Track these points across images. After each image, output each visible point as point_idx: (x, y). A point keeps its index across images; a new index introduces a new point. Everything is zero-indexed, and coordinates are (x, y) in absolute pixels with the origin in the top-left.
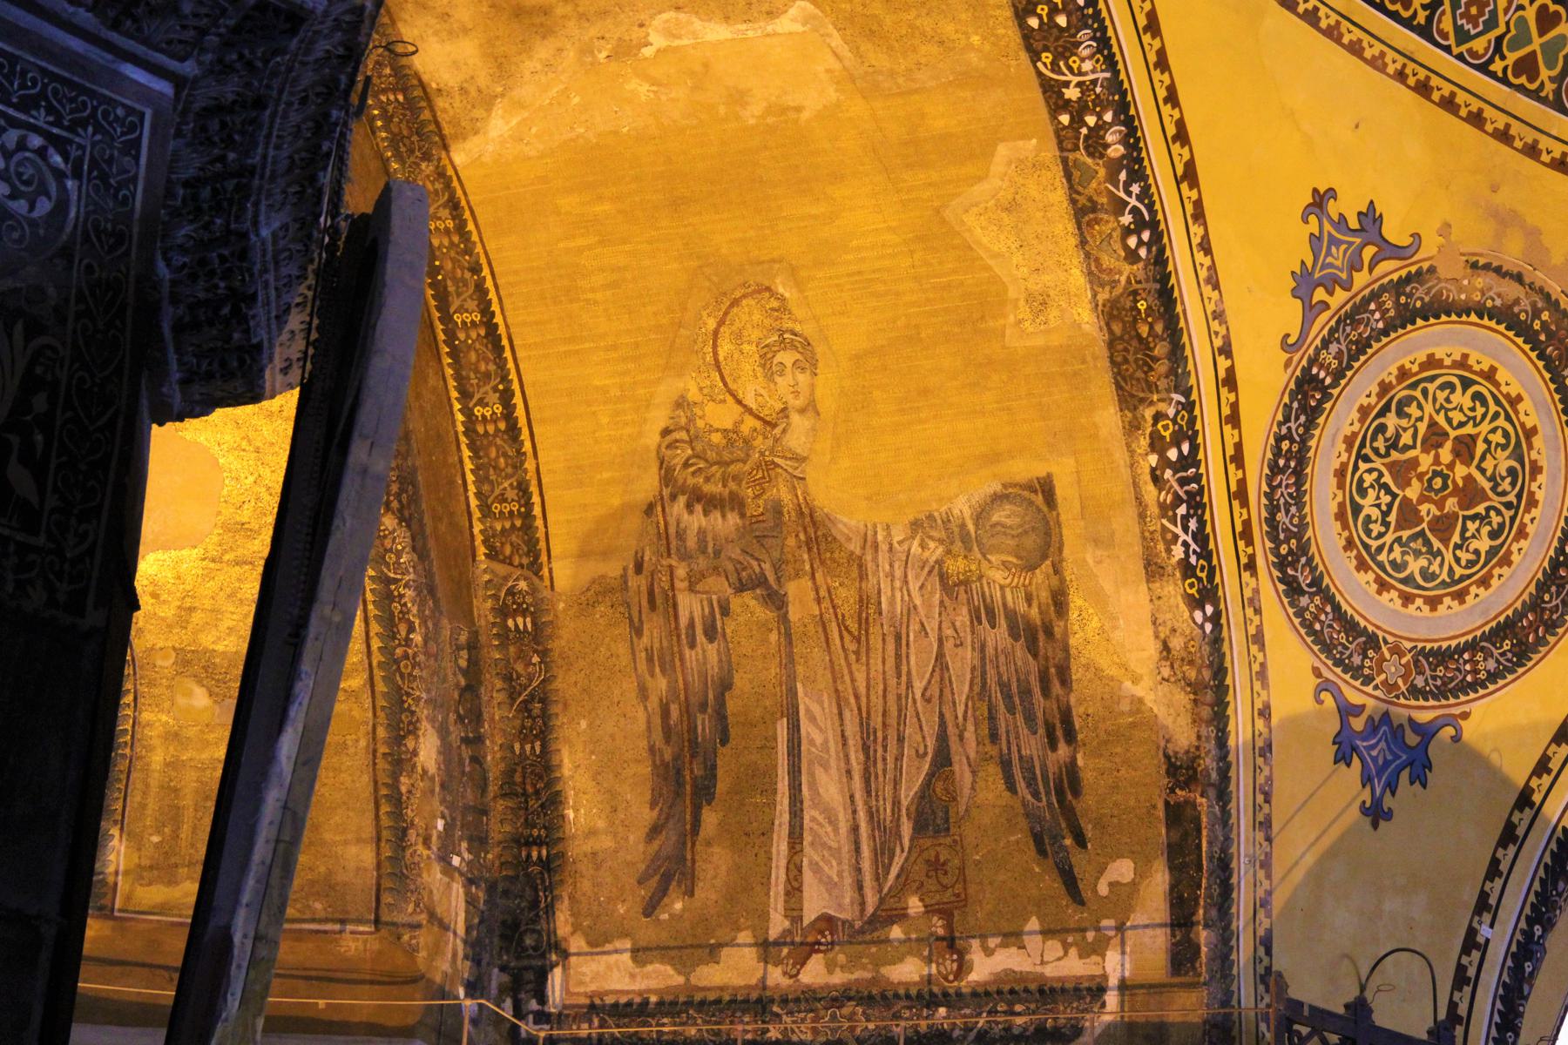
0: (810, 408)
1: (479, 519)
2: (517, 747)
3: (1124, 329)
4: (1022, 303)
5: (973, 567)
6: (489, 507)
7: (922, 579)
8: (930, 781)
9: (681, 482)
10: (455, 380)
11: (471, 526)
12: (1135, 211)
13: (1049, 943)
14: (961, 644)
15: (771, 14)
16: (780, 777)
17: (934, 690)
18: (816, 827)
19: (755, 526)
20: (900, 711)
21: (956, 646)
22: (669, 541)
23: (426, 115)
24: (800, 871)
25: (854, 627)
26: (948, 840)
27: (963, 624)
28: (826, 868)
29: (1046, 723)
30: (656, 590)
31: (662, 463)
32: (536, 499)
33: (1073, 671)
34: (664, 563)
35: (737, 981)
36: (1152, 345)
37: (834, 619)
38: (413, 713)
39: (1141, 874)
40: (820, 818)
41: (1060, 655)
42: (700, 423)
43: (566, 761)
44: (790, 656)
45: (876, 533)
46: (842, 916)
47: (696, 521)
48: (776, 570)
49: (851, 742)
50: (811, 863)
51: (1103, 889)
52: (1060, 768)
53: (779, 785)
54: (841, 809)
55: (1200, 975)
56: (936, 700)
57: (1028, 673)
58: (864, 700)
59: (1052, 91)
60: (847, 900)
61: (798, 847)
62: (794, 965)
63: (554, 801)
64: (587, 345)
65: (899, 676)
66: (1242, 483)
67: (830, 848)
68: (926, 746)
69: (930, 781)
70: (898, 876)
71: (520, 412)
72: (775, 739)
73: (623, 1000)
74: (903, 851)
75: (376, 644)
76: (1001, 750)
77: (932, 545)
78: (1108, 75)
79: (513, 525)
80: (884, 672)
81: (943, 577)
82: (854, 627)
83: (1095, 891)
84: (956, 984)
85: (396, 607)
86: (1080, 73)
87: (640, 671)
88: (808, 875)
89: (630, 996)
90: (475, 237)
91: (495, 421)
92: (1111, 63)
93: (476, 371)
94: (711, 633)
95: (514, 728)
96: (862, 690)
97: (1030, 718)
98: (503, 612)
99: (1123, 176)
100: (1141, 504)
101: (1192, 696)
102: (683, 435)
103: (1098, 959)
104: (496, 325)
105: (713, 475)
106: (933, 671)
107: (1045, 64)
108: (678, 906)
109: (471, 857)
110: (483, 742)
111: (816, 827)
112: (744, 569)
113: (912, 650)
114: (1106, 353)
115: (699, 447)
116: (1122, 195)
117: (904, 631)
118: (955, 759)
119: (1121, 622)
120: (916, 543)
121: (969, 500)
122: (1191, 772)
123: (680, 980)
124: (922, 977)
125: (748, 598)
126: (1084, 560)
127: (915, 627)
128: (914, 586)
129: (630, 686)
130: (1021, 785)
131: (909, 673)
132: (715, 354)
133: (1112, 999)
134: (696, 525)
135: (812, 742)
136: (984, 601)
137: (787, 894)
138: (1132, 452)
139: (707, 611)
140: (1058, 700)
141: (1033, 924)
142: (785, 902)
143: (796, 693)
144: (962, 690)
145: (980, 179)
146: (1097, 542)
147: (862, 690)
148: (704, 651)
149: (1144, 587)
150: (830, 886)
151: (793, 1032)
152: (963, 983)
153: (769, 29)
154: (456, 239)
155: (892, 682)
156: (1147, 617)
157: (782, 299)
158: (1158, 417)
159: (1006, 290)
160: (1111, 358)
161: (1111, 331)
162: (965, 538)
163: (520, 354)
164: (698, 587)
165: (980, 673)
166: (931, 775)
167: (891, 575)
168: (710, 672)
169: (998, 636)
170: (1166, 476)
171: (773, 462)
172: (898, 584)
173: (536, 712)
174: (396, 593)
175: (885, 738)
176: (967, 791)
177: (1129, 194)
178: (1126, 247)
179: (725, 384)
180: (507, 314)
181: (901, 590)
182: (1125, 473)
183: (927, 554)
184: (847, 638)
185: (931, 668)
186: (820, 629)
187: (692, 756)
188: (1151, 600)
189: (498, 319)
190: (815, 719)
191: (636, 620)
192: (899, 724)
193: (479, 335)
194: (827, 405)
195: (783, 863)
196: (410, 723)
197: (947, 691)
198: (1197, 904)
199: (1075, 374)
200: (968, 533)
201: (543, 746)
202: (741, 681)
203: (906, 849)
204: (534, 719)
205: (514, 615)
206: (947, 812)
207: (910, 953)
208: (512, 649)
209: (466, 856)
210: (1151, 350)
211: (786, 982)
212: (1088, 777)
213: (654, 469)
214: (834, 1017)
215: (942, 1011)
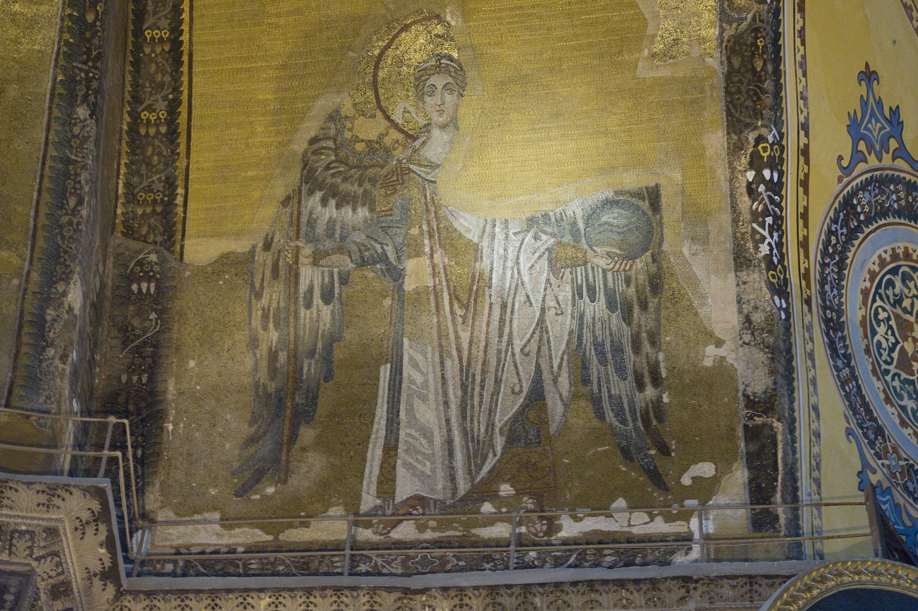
1: (123, 203)
3: (742, 64)
5: (580, 255)
6: (134, 195)
7: (533, 261)
9: (320, 179)
10: (131, 85)
11: (116, 207)
14: (562, 313)
16: (379, 405)
17: (533, 347)
18: (411, 440)
19: (382, 219)
21: (557, 314)
24: (394, 468)
25: (464, 297)
28: (419, 466)
29: (636, 373)
30: (281, 264)
31: (305, 166)
32: (180, 191)
33: (662, 337)
34: (292, 244)
36: (763, 78)
37: (445, 289)
38: (67, 266)
41: (652, 324)
42: (348, 135)
45: (494, 226)
48: (397, 251)
49: (450, 382)
51: (686, 480)
54: (437, 428)
55: (780, 531)
57: (622, 336)
58: (465, 353)
62: (384, 528)
64: (259, 64)
65: (501, 336)
66: (806, 238)
68: (521, 386)
69: (523, 410)
70: (490, 472)
71: (183, 119)
72: (378, 379)
74: (495, 455)
77: (544, 237)
79: (154, 210)
80: (487, 333)
83: (678, 481)
84: (546, 538)
85: (70, 184)
87: (254, 323)
88: (401, 471)
93: (152, 81)
96: (465, 346)
97: (620, 370)
100: (735, 212)
101: (770, 355)
102: (330, 144)
103: (684, 523)
105: (351, 176)
106: (534, 333)
111: (411, 440)
112: (368, 250)
113: (516, 315)
115: (342, 154)
120: (530, 235)
122: (768, 405)
126: (681, 252)
127: (521, 298)
128: (524, 266)
130: (610, 416)
131: (510, 335)
132: (375, 75)
134: (327, 216)
135: (413, 382)
136: (587, 280)
138: (733, 169)
139: (327, 280)
140: (647, 356)
143: (402, 345)
144: (559, 347)
146: (693, 239)
147: (465, 346)
148: (318, 310)
150: (422, 477)
151: (383, 567)
156: (732, 297)
158: (760, 139)
159: (646, 26)
160: (726, 88)
162: (575, 232)
163: (196, 69)
164: (321, 262)
168: (321, 327)
169: (597, 309)
170: (760, 190)
172: (510, 264)
174: (72, 172)
175: (483, 381)
180: (194, 33)
182: (725, 186)
183: (539, 243)
184: (456, 306)
185: (531, 331)
188: (738, 285)
189: (185, 37)
190: (418, 365)
192: (497, 371)
193: (163, 50)
195: (377, 463)
196: (64, 273)
197: (545, 349)
198: (774, 489)
199: (693, 102)
201: (151, 379)
203: (499, 454)
204: (144, 358)
205: (139, 281)
210: (762, 82)
213: (298, 169)
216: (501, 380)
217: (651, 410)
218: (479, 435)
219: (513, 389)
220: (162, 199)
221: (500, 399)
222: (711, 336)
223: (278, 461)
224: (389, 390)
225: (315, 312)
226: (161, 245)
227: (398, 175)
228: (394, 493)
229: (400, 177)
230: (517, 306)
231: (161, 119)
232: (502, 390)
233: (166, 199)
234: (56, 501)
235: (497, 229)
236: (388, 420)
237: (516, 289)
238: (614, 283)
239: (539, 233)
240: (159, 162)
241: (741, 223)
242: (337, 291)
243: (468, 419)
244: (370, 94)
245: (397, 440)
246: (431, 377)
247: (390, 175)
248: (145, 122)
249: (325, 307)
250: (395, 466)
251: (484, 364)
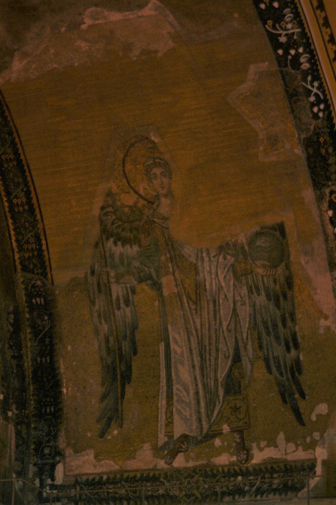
0: (169, 194)
2: (39, 359)
4: (265, 141)
5: (248, 267)
6: (22, 246)
8: (231, 370)
11: (14, 256)
12: (316, 95)
13: (289, 444)
15: (141, 7)
17: (232, 326)
18: (179, 393)
20: (216, 337)
21: (242, 305)
24: (172, 414)
25: (193, 297)
26: (241, 397)
27: (245, 294)
28: (184, 412)
29: (285, 340)
31: (101, 223)
32: (43, 242)
34: (105, 270)
35: (143, 466)
37: (184, 294)
40: (181, 388)
42: (118, 203)
43: (62, 365)
45: (202, 253)
46: (192, 434)
47: (118, 250)
48: (157, 271)
49: (194, 352)
50: (177, 409)
51: (314, 418)
52: (292, 361)
53: (161, 374)
56: (233, 331)
58: (199, 332)
59: (274, 39)
60: (194, 427)
61: (171, 403)
62: (170, 459)
63: (57, 385)
65: (215, 320)
67: (186, 402)
68: (229, 353)
69: (231, 370)
71: (34, 201)
73: (91, 478)
74: (219, 403)
76: (264, 353)
77: (229, 257)
78: (299, 30)
80: (209, 319)
81: (235, 273)
82: (193, 297)
83: (310, 419)
84: (245, 465)
86: (286, 29)
88: (176, 417)
89: (94, 476)
90: (9, 118)
91: (23, 206)
92: (301, 24)
94: (127, 303)
95: (37, 350)
97: (277, 338)
98: (30, 296)
99: (309, 78)
102: (111, 209)
103: (312, 451)
104: (21, 160)
106: (231, 317)
107: (269, 26)
108: (116, 432)
109: (17, 412)
110: (22, 358)
112: (142, 271)
113: (221, 307)
114: (306, 163)
116: (309, 87)
117: (217, 298)
119: (318, 291)
121: (245, 236)
124: (230, 462)
126: (300, 262)
127: (222, 296)
128: (221, 277)
130: (274, 369)
131: (220, 318)
132: (124, 170)
133: (319, 469)
134: (118, 251)
135: (176, 353)
136: (254, 283)
137: (167, 425)
138: (320, 210)
139: (125, 292)
141: (281, 437)
142: (166, 429)
144: (245, 326)
145: (242, 82)
148: (124, 311)
149: (328, 274)
152: (249, 465)
153: (140, 14)
157: (153, 142)
161: (308, 153)
164: (121, 281)
165: (253, 317)
167: (210, 272)
168: (127, 321)
169: (261, 300)
171: (153, 221)
172: (213, 276)
173: (47, 342)
175: (210, 350)
176: (249, 373)
177: (313, 87)
179: (129, 184)
181: (215, 279)
182: (318, 219)
183: (226, 262)
186: (178, 299)
187: (121, 361)
188: (332, 280)
191: (92, 297)
192: (216, 343)
195: (164, 410)
200: (245, 251)
201: (51, 359)
203: (221, 402)
205: (35, 297)
206: (240, 384)
208: (35, 313)
209: (16, 412)
210: (327, 160)
211: (166, 466)
213: (99, 226)
214: (189, 483)
215: (240, 478)
216: (219, 350)
217: (294, 365)
218: (211, 389)
219: (225, 356)
220: (36, 247)
221: (219, 362)
222: (322, 313)
223: (117, 410)
224: (165, 359)
225: (122, 312)
226: (41, 275)
227: (149, 225)
228: (173, 432)
229: (149, 226)
230: (221, 301)
231: (23, 202)
232: (220, 356)
233: (37, 247)
235: (204, 255)
236: (167, 380)
237: (219, 290)
238: (268, 283)
239: (226, 255)
240: (29, 226)
241: (329, 242)
242: (131, 298)
243: (205, 376)
245: (172, 393)
246: (184, 348)
247: (145, 226)
248: (16, 205)
249: (127, 309)
250: (172, 412)
251: (209, 339)
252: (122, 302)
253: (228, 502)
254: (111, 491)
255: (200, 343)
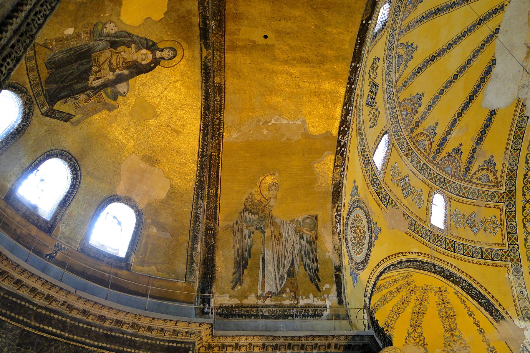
22: (243, 219)
23: (221, 131)
24: (264, 282)
32: (218, 209)
39: (331, 287)
42: (254, 198)
44: (265, 243)
51: (324, 289)
59: (339, 142)
71: (219, 192)
75: (192, 225)
88: (266, 284)
90: (221, 157)
91: (213, 193)
96: (278, 250)
97: (309, 258)
102: (250, 200)
115: (252, 203)
118: (295, 264)
123: (240, 302)
125: (258, 231)
127: (289, 239)
128: (290, 232)
129: (231, 246)
130: (308, 270)
135: (267, 259)
144: (297, 252)
145: (320, 158)
146: (324, 227)
147: (278, 250)
150: (271, 286)
154: (217, 157)
155: (284, 249)
158: (338, 206)
161: (333, 189)
165: (300, 249)
166: (290, 267)
169: (304, 242)
176: (297, 270)
178: (341, 174)
187: (243, 260)
189: (220, 174)
194: (279, 197)
195: (261, 281)
197: (294, 252)
202: (254, 246)
207: (287, 299)
211: (262, 303)
212: (320, 269)
214: (273, 310)
234: (201, 326)
244: (259, 189)
252: (247, 236)
253: (290, 319)
254: (237, 311)
255: (278, 256)
